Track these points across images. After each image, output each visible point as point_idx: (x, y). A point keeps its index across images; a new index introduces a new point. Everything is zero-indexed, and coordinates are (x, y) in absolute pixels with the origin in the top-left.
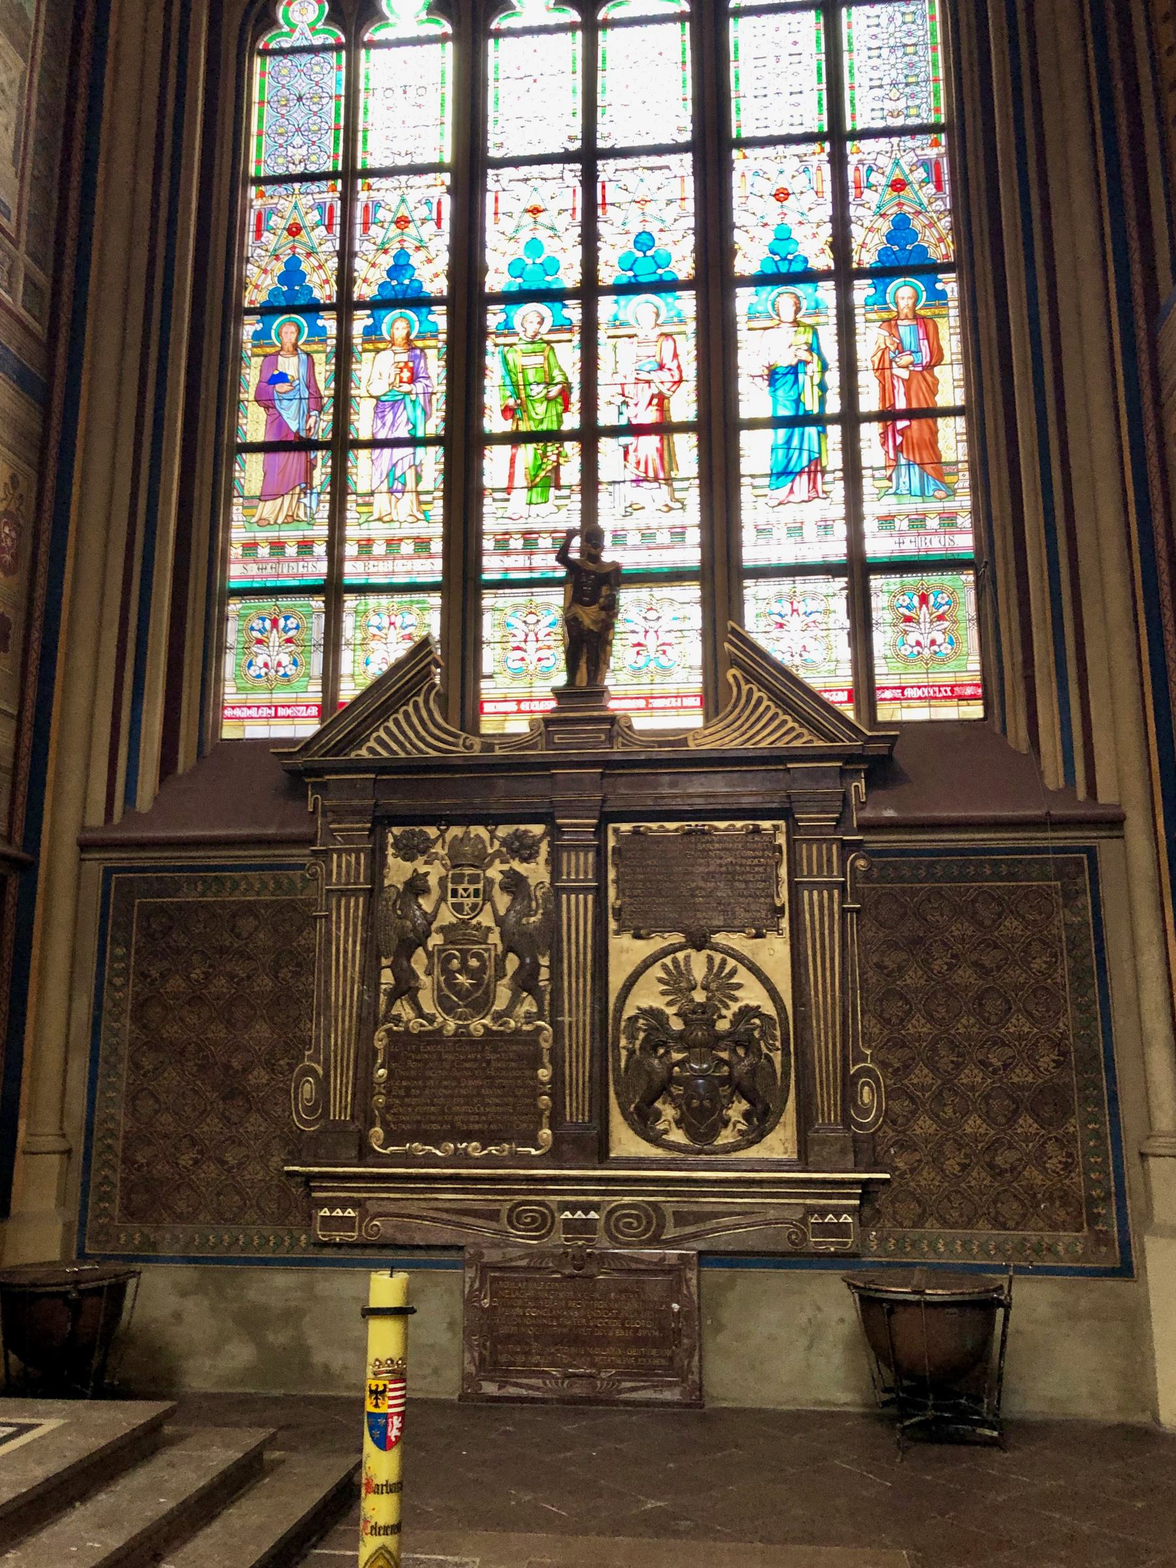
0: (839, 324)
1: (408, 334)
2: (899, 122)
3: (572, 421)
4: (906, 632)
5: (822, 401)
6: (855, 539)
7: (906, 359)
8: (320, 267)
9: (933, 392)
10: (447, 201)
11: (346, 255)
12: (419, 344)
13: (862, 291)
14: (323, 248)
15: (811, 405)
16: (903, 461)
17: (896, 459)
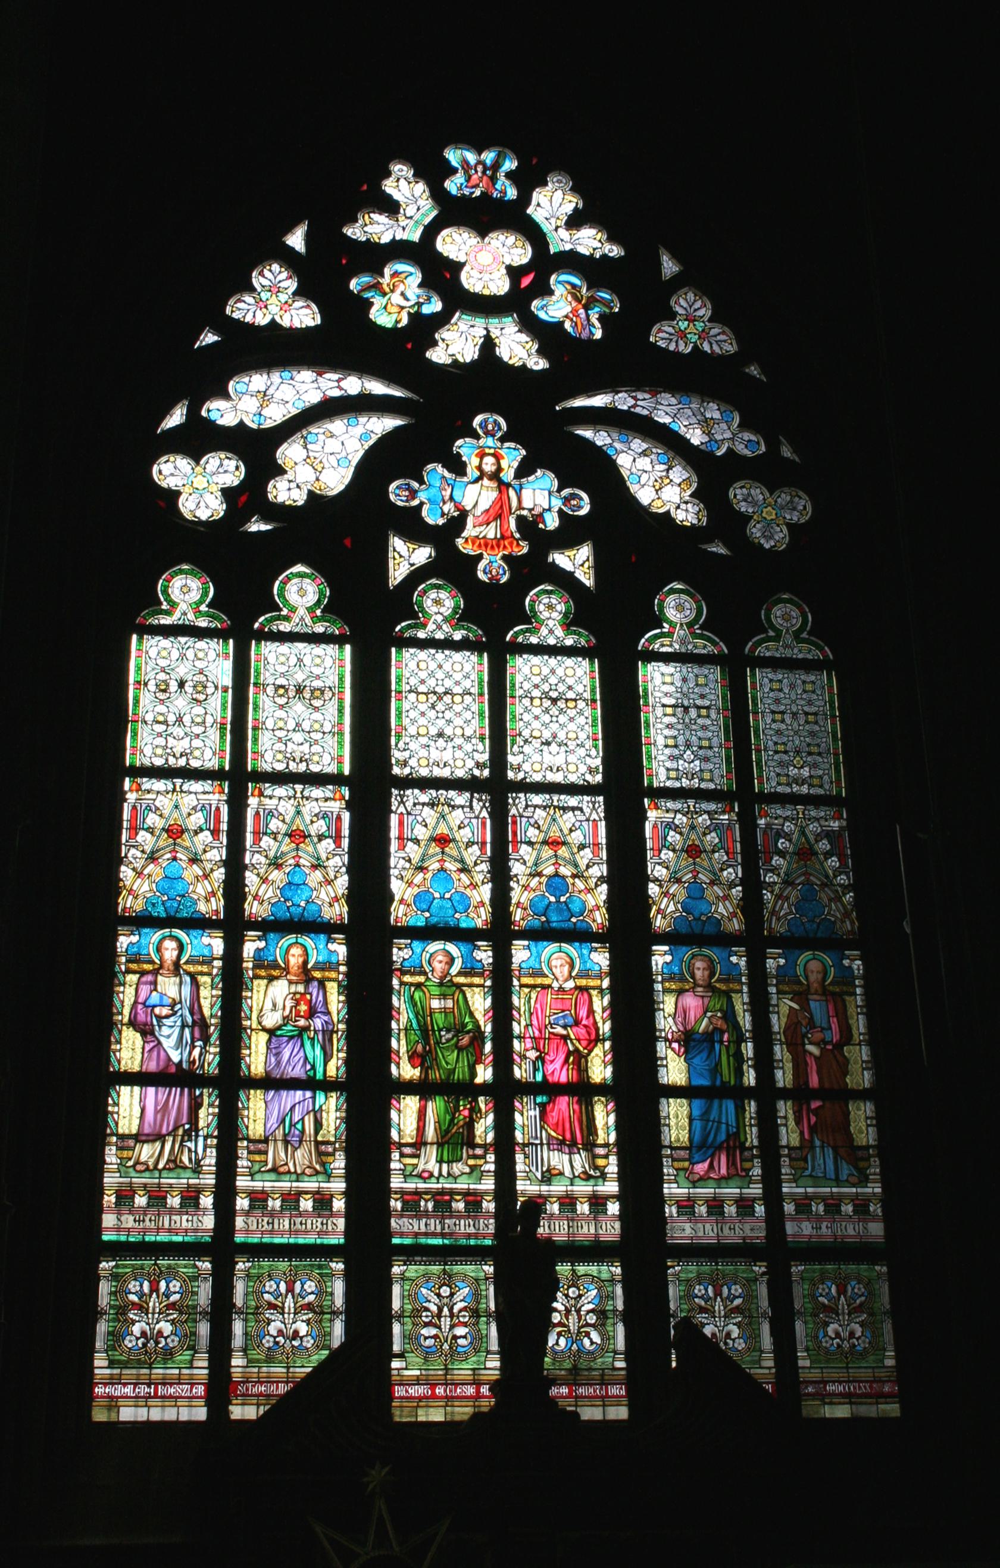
1: (305, 962)
2: (805, 789)
3: (484, 1074)
4: (827, 1324)
5: (739, 1073)
6: (775, 1219)
8: (206, 876)
9: (845, 1073)
10: (346, 817)
11: (235, 866)
12: (317, 974)
14: (208, 856)
16: (817, 1143)
17: (812, 1141)
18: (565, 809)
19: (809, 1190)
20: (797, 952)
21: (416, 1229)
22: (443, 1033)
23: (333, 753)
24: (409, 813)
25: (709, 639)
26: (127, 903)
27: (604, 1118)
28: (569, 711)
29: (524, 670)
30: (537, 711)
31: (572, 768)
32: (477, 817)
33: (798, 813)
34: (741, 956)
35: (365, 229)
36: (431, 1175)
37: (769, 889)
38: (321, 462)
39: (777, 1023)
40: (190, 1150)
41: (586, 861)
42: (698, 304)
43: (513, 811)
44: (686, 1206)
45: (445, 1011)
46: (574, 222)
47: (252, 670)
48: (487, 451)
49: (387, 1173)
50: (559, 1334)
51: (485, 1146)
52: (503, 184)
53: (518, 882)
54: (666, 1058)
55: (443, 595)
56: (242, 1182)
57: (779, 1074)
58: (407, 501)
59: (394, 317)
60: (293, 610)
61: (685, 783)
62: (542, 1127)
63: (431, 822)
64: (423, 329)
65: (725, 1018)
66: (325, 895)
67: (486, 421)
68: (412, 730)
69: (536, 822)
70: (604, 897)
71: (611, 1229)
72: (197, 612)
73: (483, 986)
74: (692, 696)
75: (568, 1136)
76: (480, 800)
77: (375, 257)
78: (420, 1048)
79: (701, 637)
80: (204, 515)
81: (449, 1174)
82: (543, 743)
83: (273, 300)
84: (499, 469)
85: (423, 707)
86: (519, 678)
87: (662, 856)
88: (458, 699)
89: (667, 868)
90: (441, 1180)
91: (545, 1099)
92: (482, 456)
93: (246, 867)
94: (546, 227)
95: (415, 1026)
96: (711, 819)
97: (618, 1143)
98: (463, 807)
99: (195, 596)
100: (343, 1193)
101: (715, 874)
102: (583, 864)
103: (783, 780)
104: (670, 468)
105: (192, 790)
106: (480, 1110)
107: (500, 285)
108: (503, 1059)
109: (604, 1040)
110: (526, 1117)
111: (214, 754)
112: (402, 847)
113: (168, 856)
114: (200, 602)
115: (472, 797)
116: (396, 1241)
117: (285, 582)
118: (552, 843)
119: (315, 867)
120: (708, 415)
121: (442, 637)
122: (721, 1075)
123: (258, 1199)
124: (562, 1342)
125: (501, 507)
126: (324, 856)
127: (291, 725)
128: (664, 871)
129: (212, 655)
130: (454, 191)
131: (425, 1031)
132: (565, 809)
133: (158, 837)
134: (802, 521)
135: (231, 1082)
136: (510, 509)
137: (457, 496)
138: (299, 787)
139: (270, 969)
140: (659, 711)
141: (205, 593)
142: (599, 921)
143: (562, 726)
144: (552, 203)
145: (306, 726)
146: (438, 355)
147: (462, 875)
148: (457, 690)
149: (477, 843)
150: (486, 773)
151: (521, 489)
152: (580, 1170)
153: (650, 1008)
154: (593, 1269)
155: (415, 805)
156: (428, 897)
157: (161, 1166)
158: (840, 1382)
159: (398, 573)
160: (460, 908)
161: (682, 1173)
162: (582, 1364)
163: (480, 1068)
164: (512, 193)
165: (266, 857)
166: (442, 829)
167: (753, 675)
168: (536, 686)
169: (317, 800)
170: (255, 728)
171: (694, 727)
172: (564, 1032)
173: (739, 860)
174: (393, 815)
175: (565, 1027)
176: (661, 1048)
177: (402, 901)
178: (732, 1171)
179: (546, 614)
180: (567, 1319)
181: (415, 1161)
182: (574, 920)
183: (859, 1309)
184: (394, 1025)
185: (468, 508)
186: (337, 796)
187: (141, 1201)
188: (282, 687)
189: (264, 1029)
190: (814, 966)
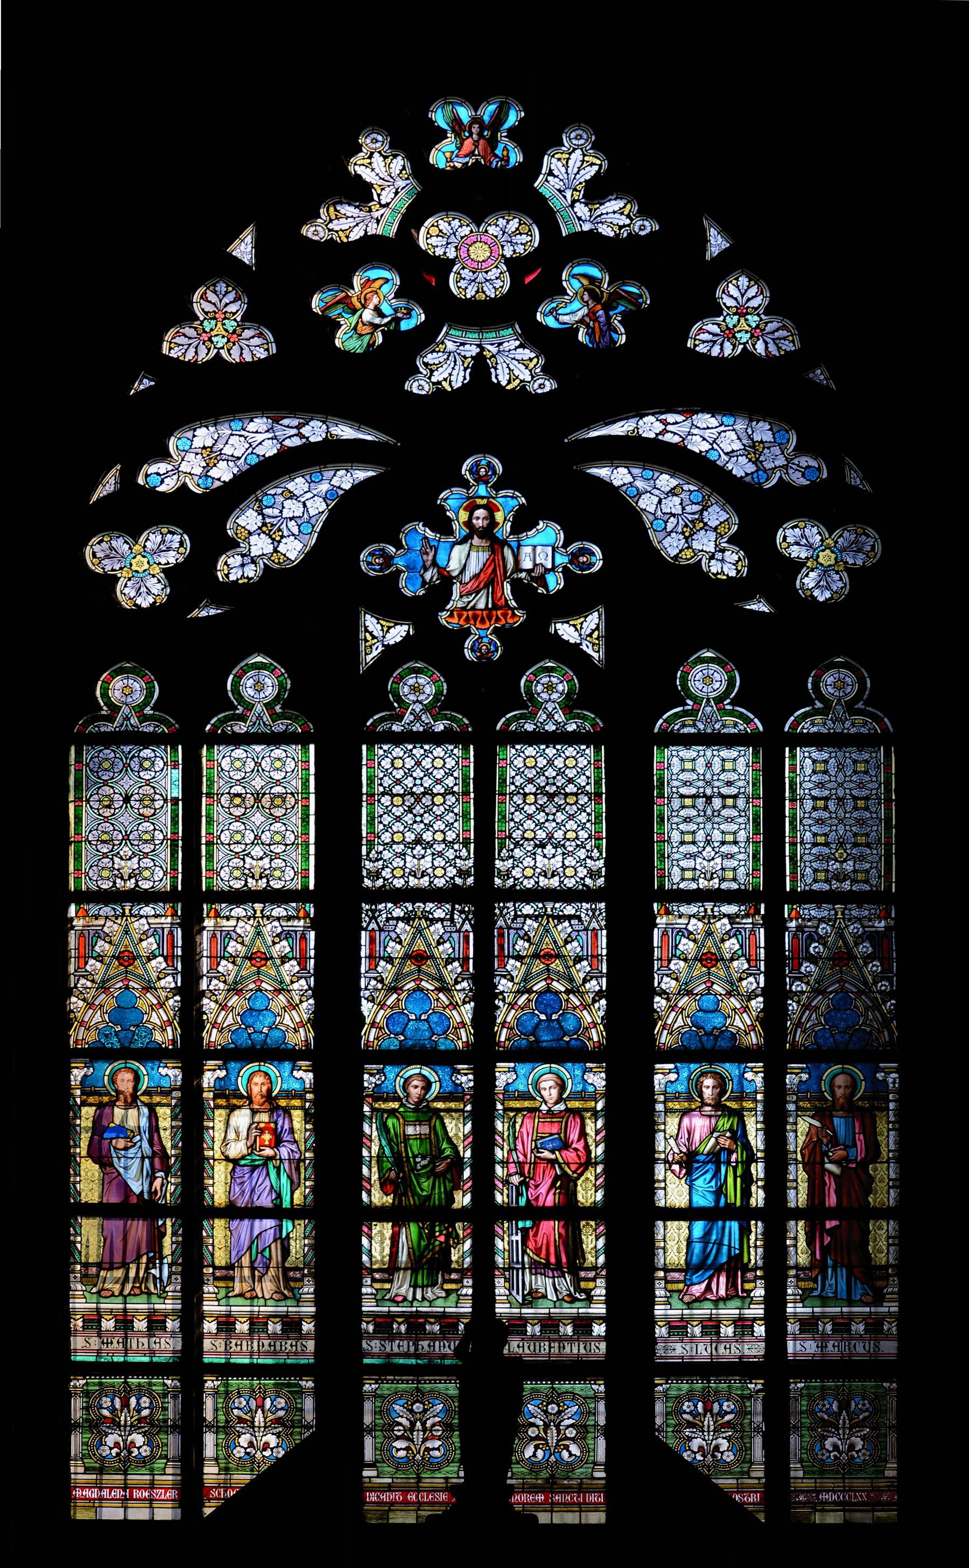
1: (270, 1091)
3: (463, 1200)
5: (746, 1194)
6: (776, 1337)
9: (869, 1191)
11: (190, 993)
12: (283, 1103)
14: (162, 983)
15: (733, 1195)
16: (830, 1262)
18: (561, 918)
19: (816, 1310)
20: (823, 1065)
21: (388, 1350)
22: (418, 1160)
23: (295, 868)
24: (381, 930)
25: (741, 716)
27: (593, 1242)
28: (568, 808)
29: (517, 762)
30: (530, 809)
31: (570, 872)
32: (459, 931)
33: (836, 914)
34: (757, 1073)
35: (330, 226)
36: (405, 1299)
37: (796, 998)
38: (279, 530)
40: (154, 1276)
41: (582, 975)
42: (753, 291)
43: (500, 923)
44: (678, 1328)
45: (420, 1137)
46: (595, 192)
47: (204, 779)
48: (479, 502)
49: (359, 1297)
50: (537, 1447)
51: (462, 1272)
52: (505, 148)
53: (504, 1000)
54: (665, 1181)
57: (791, 1194)
58: (380, 570)
59: (367, 338)
60: (249, 707)
61: (703, 884)
62: (524, 1252)
64: (402, 350)
65: (734, 1138)
67: (477, 464)
68: (386, 837)
69: (526, 934)
70: (601, 1013)
72: (143, 718)
73: (463, 1111)
74: (716, 784)
75: (553, 1260)
76: (462, 912)
77: (343, 260)
78: (393, 1175)
79: (731, 713)
80: (145, 602)
81: (424, 1298)
82: (536, 846)
83: (217, 329)
84: (493, 523)
85: (398, 811)
87: (672, 966)
88: (439, 800)
89: (677, 979)
90: (415, 1304)
91: (528, 1224)
92: (471, 509)
93: (202, 994)
94: (557, 203)
95: (387, 1151)
96: (731, 924)
97: (606, 1265)
98: (442, 920)
99: (138, 697)
100: (312, 1317)
101: (732, 984)
103: (821, 876)
104: (705, 508)
105: (142, 913)
106: (457, 1235)
107: (497, 283)
108: (484, 1183)
109: (596, 1164)
111: (165, 873)
112: (373, 967)
113: (120, 984)
114: (145, 703)
115: (453, 908)
116: (366, 1361)
117: (239, 677)
118: (544, 956)
119: (278, 991)
120: (757, 437)
121: (421, 729)
122: (726, 1196)
124: (540, 1454)
125: (494, 571)
126: (288, 979)
127: (250, 837)
128: (673, 983)
129: (160, 764)
130: (442, 164)
131: (399, 1160)
132: (561, 918)
133: (109, 965)
134: (868, 564)
135: (193, 1210)
136: (505, 571)
137: (441, 559)
138: (259, 906)
139: (230, 1098)
140: (676, 803)
141: (150, 694)
142: (596, 1039)
143: (560, 825)
144: (569, 167)
146: (418, 386)
147: (441, 995)
148: (438, 789)
149: (458, 959)
150: (470, 880)
151: (519, 546)
152: (565, 1293)
153: (649, 1129)
154: (578, 1387)
155: (388, 920)
156: (402, 1019)
157: (126, 1292)
158: (834, 1492)
160: (438, 1030)
161: (675, 1295)
162: (559, 1473)
163: (458, 1196)
164: (516, 157)
165: (225, 982)
166: (420, 945)
167: (793, 756)
168: (530, 781)
169: (278, 919)
170: (209, 844)
171: (717, 819)
172: (553, 1157)
173: (763, 969)
174: (363, 933)
175: (553, 1152)
177: (373, 1024)
178: (731, 1292)
179: (545, 696)
180: (546, 1433)
181: (387, 1286)
182: (566, 1039)
183: (861, 1424)
184: (365, 1153)
185: (455, 574)
186: (301, 914)
188: (239, 795)
189: (227, 1159)
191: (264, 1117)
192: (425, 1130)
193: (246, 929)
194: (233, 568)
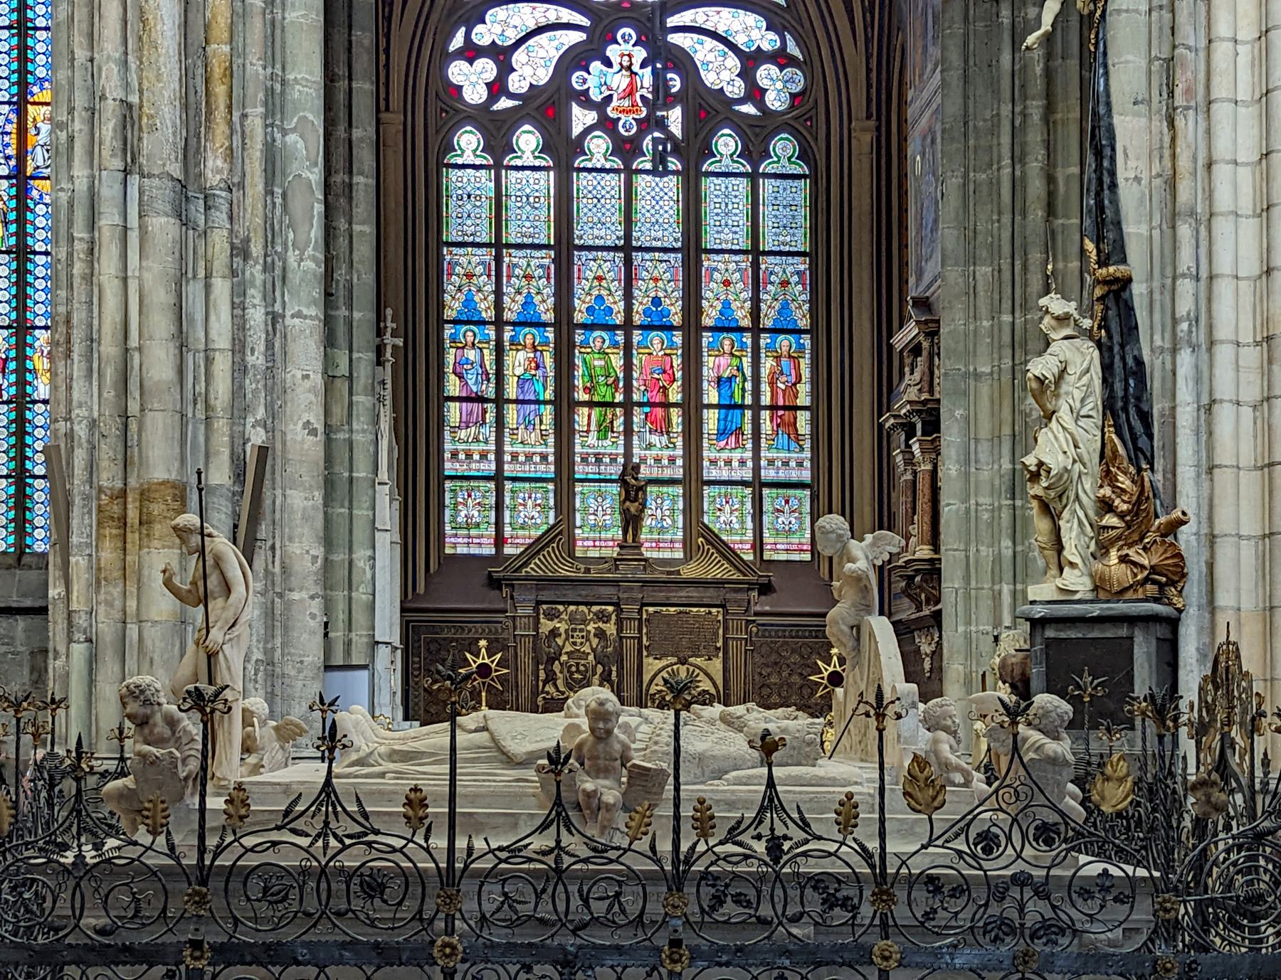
0: (752, 357)
2: (787, 248)
3: (619, 398)
5: (743, 397)
6: (757, 469)
7: (784, 379)
10: (552, 267)
11: (498, 293)
13: (765, 340)
15: (738, 400)
23: (546, 234)
26: (449, 314)
39: (765, 372)
44: (713, 462)
55: (601, 141)
56: (507, 448)
57: (763, 398)
63: (594, 269)
66: (542, 308)
68: (585, 219)
71: (679, 473)
86: (639, 189)
99: (474, 146)
102: (670, 290)
110: (638, 417)
123: (515, 456)
129: (483, 180)
135: (500, 401)
145: (531, 218)
148: (608, 196)
153: (699, 364)
159: (577, 130)
163: (617, 395)
166: (600, 273)
176: (705, 384)
187: (462, 456)
190: (786, 343)
191: (532, 355)
192: (602, 363)
193: (523, 262)
194: (517, 83)
